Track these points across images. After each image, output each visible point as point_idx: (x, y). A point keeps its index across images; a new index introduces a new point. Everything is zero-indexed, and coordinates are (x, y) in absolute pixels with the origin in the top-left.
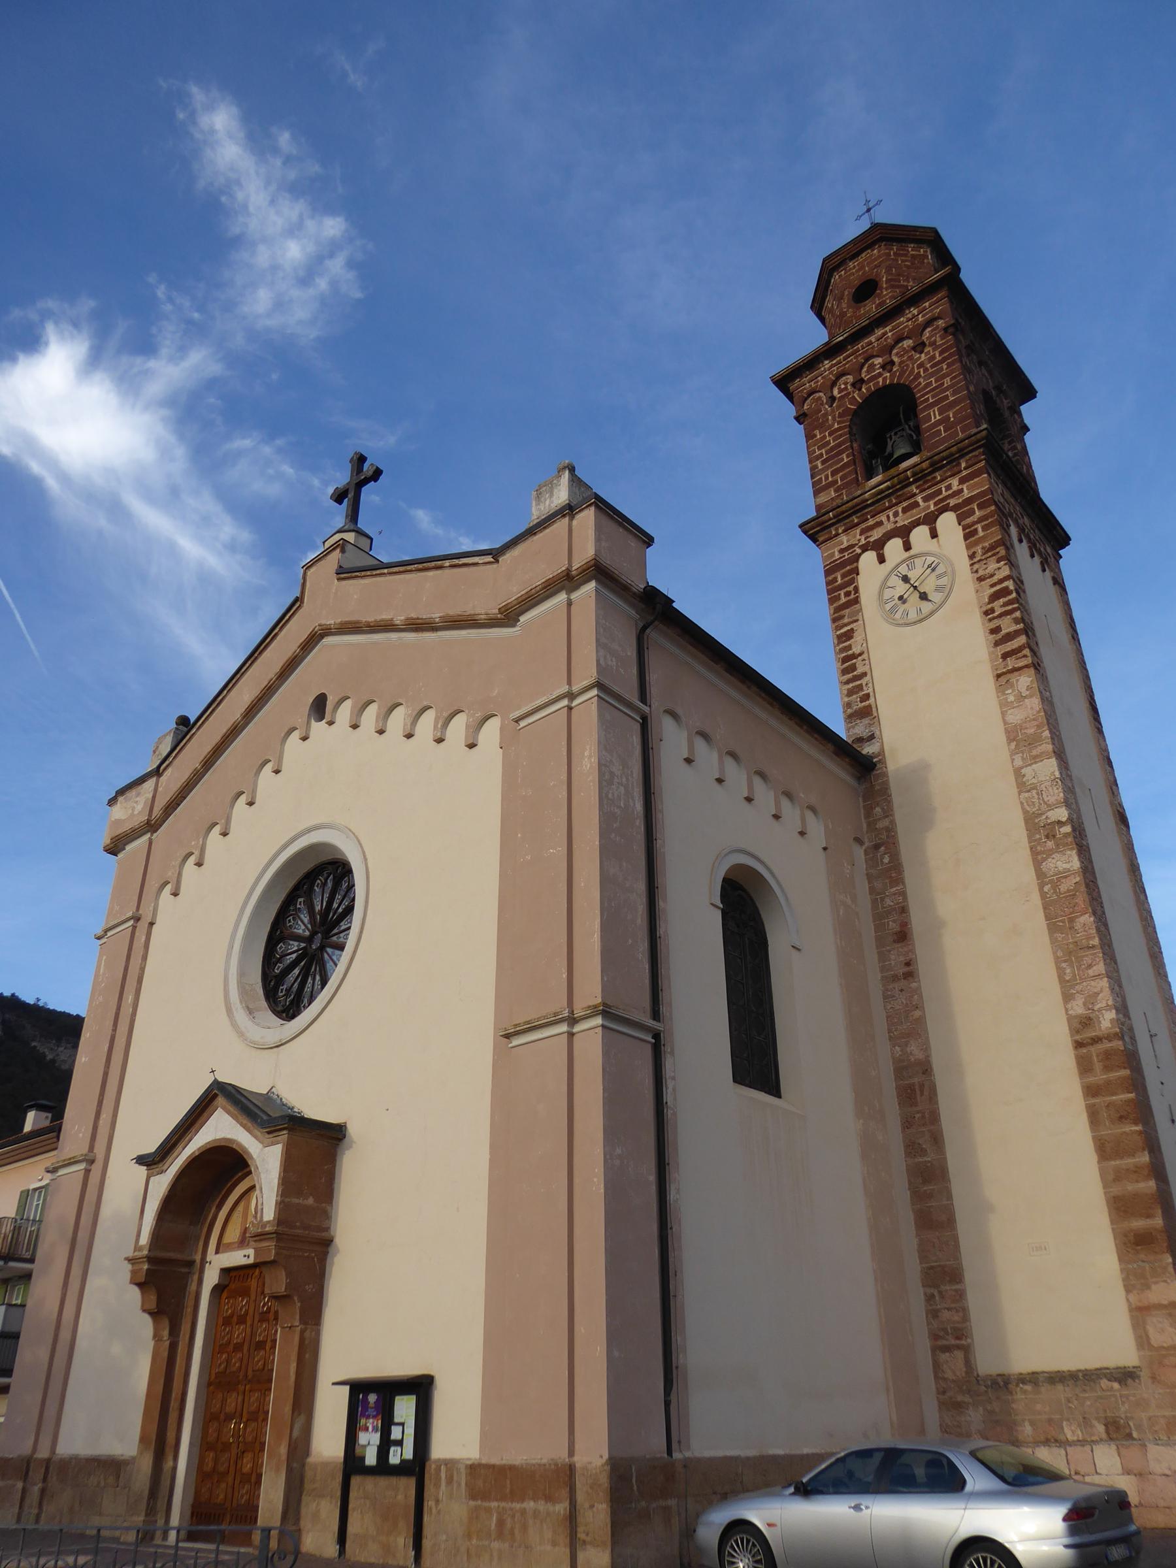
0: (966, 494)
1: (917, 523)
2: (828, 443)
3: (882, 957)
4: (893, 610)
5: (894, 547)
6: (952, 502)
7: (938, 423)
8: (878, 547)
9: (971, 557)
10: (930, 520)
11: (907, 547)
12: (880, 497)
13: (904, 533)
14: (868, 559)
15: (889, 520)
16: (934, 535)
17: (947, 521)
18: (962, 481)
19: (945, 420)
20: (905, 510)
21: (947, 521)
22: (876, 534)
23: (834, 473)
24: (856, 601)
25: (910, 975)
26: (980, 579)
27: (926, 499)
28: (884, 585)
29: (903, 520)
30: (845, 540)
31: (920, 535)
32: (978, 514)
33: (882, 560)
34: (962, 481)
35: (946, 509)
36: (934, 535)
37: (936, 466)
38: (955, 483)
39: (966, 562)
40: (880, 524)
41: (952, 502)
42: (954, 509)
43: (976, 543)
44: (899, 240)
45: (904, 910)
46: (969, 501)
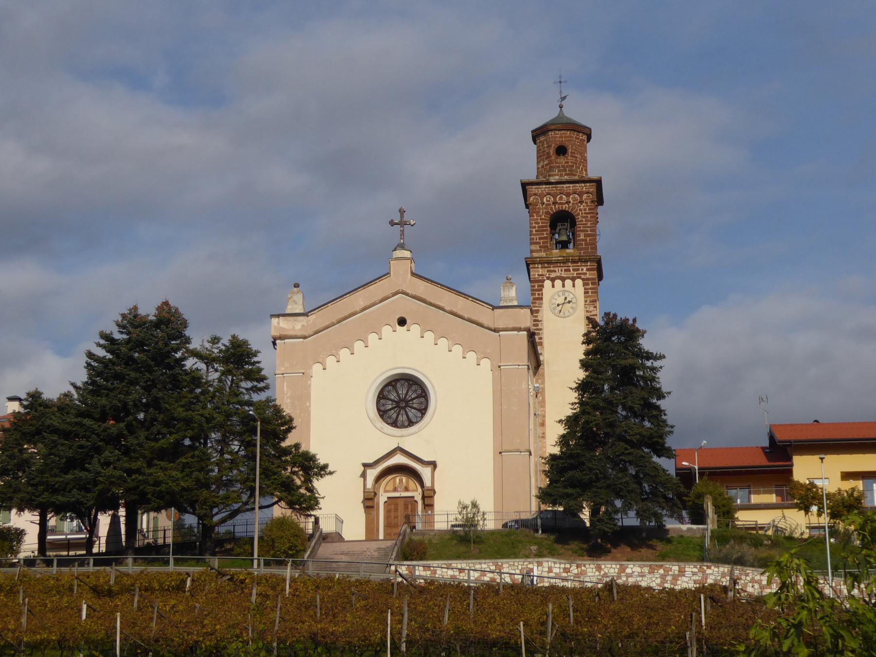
0: (588, 276)
1: (568, 278)
2: (538, 223)
3: (535, 429)
4: (554, 308)
5: (558, 283)
6: (583, 277)
7: (582, 240)
8: (553, 280)
9: (586, 301)
10: (573, 279)
11: (564, 286)
12: (557, 262)
13: (563, 279)
14: (548, 283)
15: (559, 272)
16: (574, 286)
17: (579, 282)
18: (587, 270)
19: (585, 240)
20: (565, 270)
21: (579, 282)
22: (553, 275)
23: (540, 238)
24: (541, 299)
25: (544, 437)
26: (587, 311)
27: (574, 270)
28: (552, 297)
29: (564, 274)
30: (541, 271)
31: (568, 282)
32: (590, 286)
33: (553, 286)
34: (587, 270)
35: (580, 278)
36: (574, 286)
37: (580, 260)
38: (585, 269)
39: (583, 303)
40: (555, 271)
41: (583, 277)
42: (583, 280)
43: (588, 297)
44: (575, 131)
45: (544, 416)
46: (588, 279)
